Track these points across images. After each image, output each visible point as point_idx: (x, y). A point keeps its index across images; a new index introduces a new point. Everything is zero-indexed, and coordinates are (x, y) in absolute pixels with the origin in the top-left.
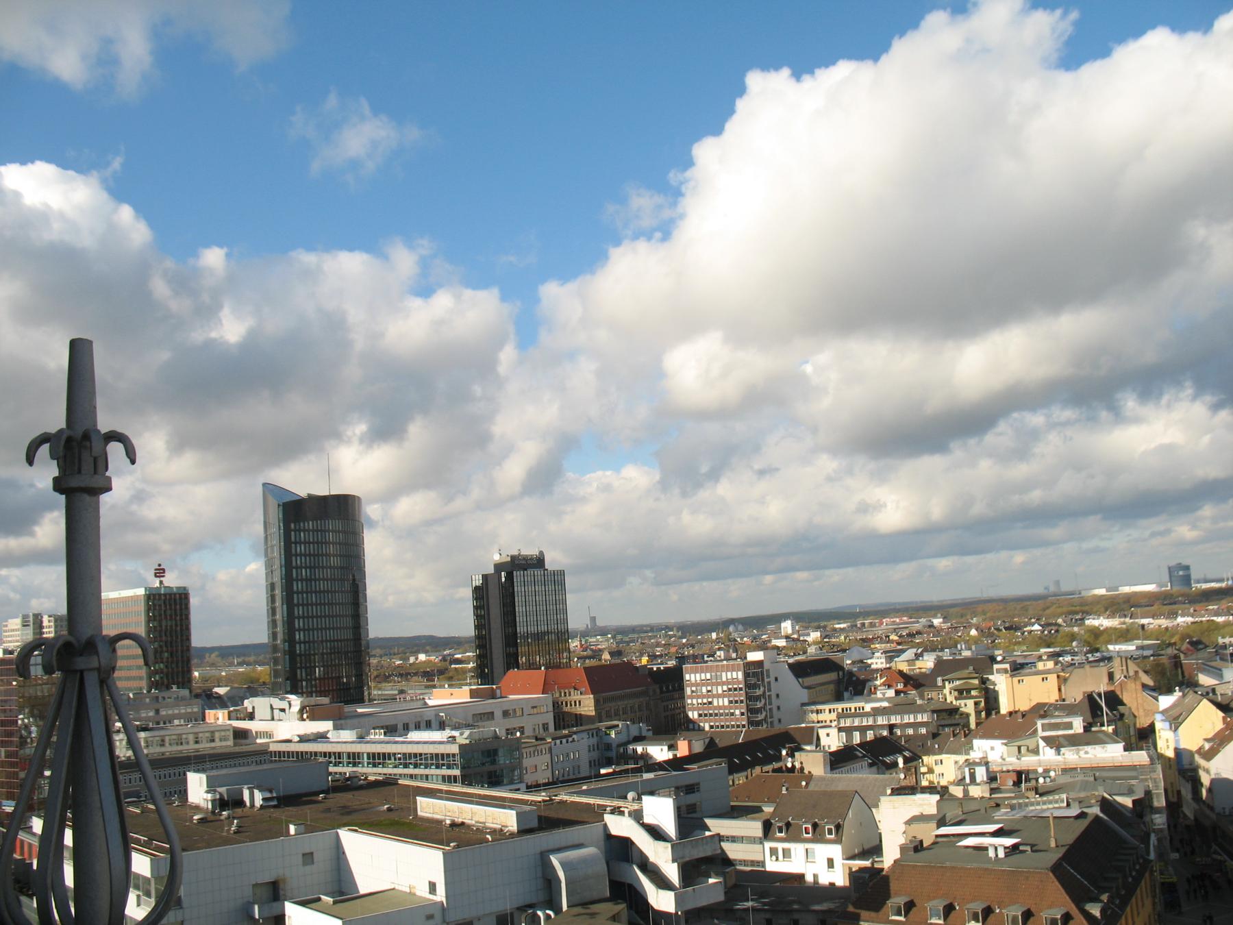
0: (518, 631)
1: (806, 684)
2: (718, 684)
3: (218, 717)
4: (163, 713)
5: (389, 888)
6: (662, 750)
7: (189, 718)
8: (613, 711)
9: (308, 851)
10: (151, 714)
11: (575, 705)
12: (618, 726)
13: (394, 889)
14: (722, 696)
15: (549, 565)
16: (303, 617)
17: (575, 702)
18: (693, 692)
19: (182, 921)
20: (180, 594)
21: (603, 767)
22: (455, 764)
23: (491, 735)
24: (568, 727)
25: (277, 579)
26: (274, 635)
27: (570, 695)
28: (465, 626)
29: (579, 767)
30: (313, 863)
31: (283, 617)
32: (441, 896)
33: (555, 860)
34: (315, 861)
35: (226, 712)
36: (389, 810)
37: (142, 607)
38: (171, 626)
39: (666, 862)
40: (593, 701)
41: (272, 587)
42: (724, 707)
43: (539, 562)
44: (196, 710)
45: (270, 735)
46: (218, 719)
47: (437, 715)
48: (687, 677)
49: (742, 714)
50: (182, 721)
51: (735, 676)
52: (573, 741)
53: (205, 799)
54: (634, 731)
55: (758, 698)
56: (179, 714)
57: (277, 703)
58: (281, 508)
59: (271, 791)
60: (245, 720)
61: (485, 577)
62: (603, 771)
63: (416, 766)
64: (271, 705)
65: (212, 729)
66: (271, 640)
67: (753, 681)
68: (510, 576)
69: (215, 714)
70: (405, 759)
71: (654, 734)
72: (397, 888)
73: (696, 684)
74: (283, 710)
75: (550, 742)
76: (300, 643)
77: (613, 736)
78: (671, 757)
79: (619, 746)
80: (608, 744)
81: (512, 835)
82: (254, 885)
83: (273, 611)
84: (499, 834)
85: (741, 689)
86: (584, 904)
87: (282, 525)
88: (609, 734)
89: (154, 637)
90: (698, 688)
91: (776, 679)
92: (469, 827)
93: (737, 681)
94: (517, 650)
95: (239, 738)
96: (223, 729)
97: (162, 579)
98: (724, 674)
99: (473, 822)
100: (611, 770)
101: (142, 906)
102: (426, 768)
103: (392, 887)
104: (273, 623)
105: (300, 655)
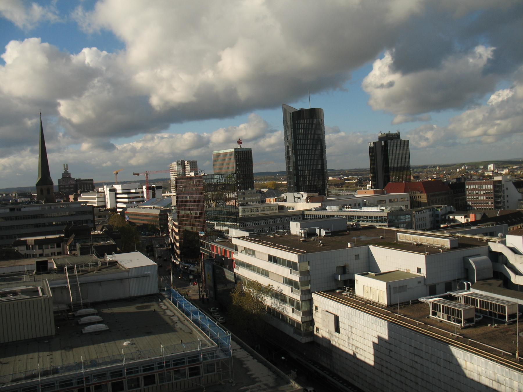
0: (389, 166)
1: (520, 191)
2: (481, 190)
3: (271, 201)
5: (396, 270)
6: (462, 218)
7: (256, 201)
8: (434, 200)
9: (357, 254)
10: (242, 199)
11: (418, 198)
12: (442, 207)
13: (398, 270)
14: (483, 195)
15: (402, 138)
16: (301, 160)
17: (418, 196)
18: (469, 193)
19: (310, 281)
21: (442, 224)
22: (385, 221)
23: (399, 209)
24: (421, 207)
25: (290, 144)
26: (289, 167)
27: (416, 193)
28: (366, 164)
29: (426, 224)
30: (359, 259)
32: (424, 273)
33: (471, 261)
34: (360, 258)
36: (382, 238)
37: (234, 156)
39: (521, 263)
40: (426, 196)
41: (288, 147)
42: (483, 200)
43: (398, 136)
44: (259, 198)
47: (363, 201)
48: (467, 187)
49: (492, 203)
50: (252, 202)
51: (489, 186)
52: (424, 213)
54: (448, 209)
55: (499, 197)
56: (253, 199)
57: (296, 195)
58: (291, 114)
59: (328, 230)
61: (375, 143)
62: (442, 226)
63: (372, 221)
64: (294, 196)
66: (288, 169)
67: (497, 189)
68: (386, 142)
70: (367, 218)
71: (457, 210)
72: (400, 270)
73: (471, 190)
74: (299, 198)
75: (414, 213)
76: (300, 171)
77: (440, 211)
78: (466, 221)
79: (442, 215)
80: (437, 215)
81: (448, 249)
82: (336, 267)
83: (288, 157)
84: (445, 250)
85: (492, 193)
86: (485, 279)
88: (438, 210)
90: (472, 192)
91: (507, 189)
92: (424, 246)
93: (491, 190)
94: (389, 174)
95: (280, 209)
96: (274, 205)
98: (484, 186)
99: (427, 244)
100: (445, 225)
102: (372, 222)
103: (397, 270)
104: (288, 163)
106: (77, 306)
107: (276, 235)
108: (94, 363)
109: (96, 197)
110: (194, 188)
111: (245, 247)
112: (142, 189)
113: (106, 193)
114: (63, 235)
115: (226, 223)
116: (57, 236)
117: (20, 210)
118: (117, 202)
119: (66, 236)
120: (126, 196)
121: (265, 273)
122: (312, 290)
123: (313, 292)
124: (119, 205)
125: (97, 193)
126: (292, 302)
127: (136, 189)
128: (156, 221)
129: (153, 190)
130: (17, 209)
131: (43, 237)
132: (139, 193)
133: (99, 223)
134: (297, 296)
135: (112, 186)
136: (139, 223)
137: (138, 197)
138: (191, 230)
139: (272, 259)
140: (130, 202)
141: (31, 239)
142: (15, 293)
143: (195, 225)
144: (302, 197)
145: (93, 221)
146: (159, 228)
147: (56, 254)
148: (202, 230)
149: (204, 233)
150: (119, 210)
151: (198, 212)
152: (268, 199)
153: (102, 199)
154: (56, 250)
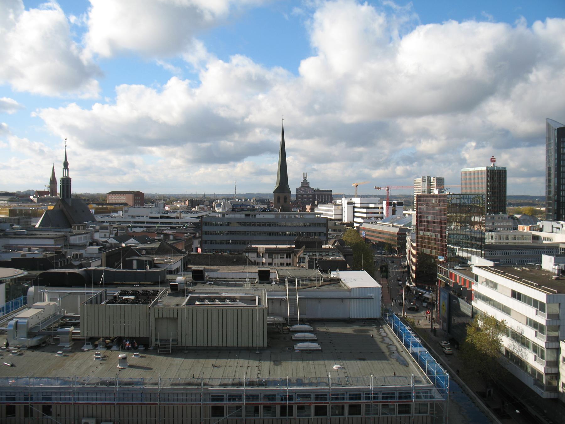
3: (524, 229)
4: (496, 224)
7: (508, 228)
10: (491, 224)
19: (559, 326)
20: (503, 170)
25: (552, 165)
26: (549, 192)
31: (555, 184)
35: (529, 226)
37: (485, 176)
38: (498, 185)
41: (549, 169)
44: (510, 224)
45: (551, 239)
46: (524, 229)
53: (553, 268)
56: (503, 225)
57: (555, 224)
58: (556, 131)
60: (537, 231)
64: (552, 226)
65: (523, 234)
69: (523, 228)
74: (559, 228)
87: (556, 139)
89: (490, 190)
96: (528, 234)
97: (494, 163)
101: (538, 315)
104: (549, 187)
105: (562, 202)
106: (294, 321)
107: (524, 268)
108: (300, 382)
109: (333, 209)
110: (437, 208)
111: (486, 279)
112: (382, 204)
113: (343, 206)
114: (293, 246)
115: (469, 249)
116: (288, 246)
117: (255, 216)
118: (354, 217)
119: (296, 247)
120: (365, 210)
121: (506, 310)
122: (560, 338)
123: (561, 340)
124: (356, 220)
125: (335, 205)
126: (535, 349)
127: (376, 204)
128: (393, 240)
129: (393, 207)
130: (252, 215)
131: (274, 246)
132: (378, 208)
133: (332, 237)
134: (541, 342)
135: (351, 199)
136: (374, 240)
137: (378, 213)
138: (429, 253)
139: (516, 295)
140: (368, 217)
141: (262, 247)
142: (233, 299)
143: (435, 248)
144: (562, 228)
145: (326, 235)
146: (396, 248)
147: (285, 265)
148: (442, 255)
149: (443, 258)
150: (355, 225)
151: (439, 235)
152: (522, 226)
153: (339, 212)
154: (285, 260)
